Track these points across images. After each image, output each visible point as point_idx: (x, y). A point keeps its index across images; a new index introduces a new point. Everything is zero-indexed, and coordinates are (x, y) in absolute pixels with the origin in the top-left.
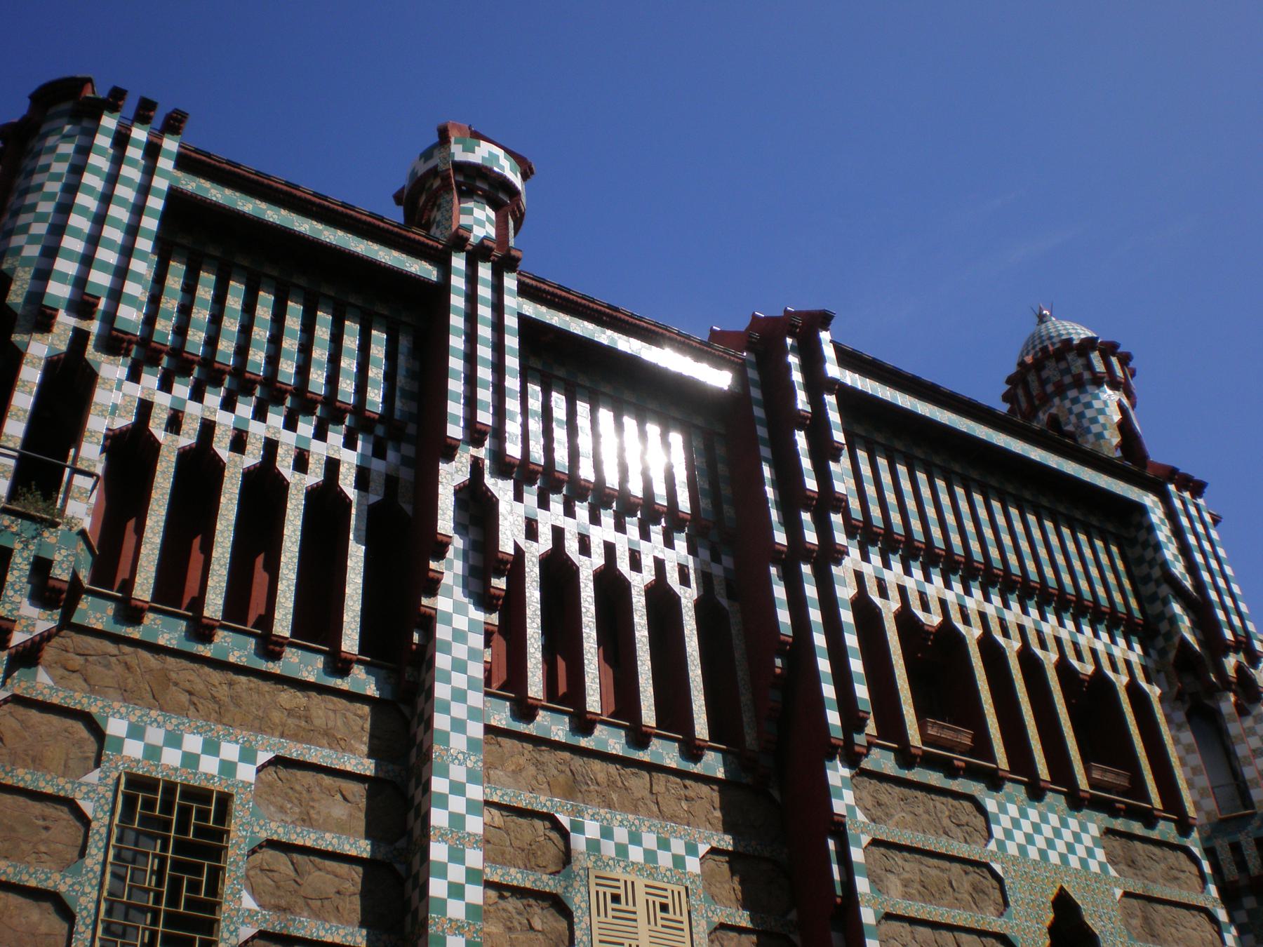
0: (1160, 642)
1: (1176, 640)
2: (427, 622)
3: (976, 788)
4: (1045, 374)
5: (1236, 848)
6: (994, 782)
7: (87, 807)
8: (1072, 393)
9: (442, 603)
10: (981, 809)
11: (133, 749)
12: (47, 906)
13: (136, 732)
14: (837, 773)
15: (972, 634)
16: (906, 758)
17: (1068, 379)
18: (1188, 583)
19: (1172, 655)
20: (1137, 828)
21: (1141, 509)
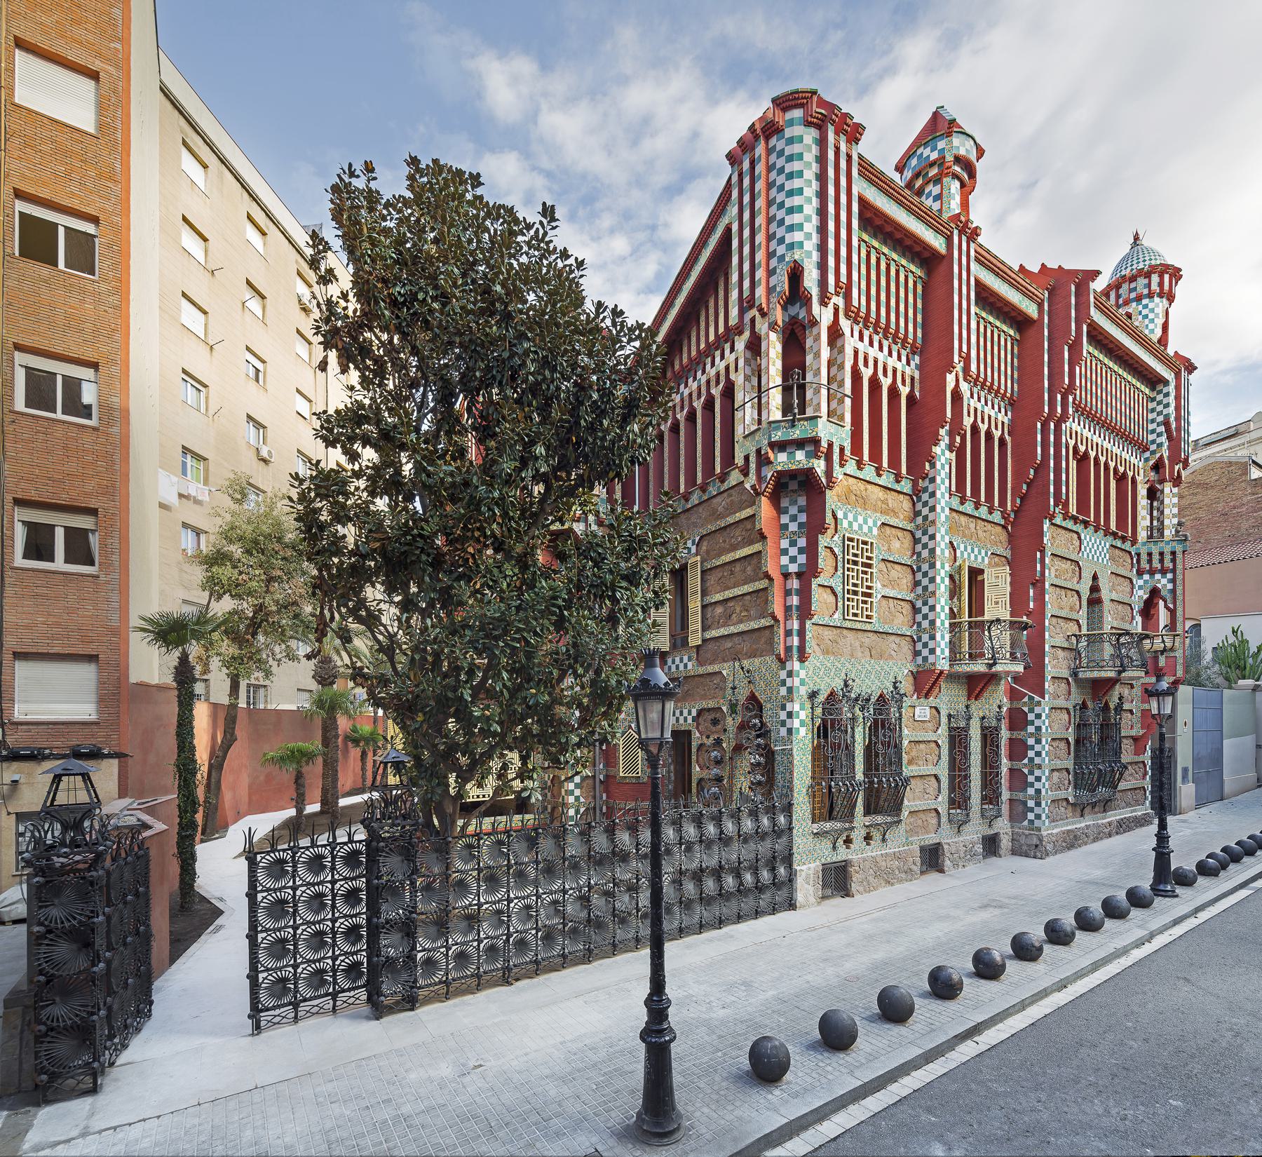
0: (1147, 454)
1: (1158, 455)
2: (932, 461)
3: (1079, 528)
4: (1133, 285)
5: (1150, 554)
6: (1086, 524)
7: (836, 550)
8: (1145, 301)
9: (937, 450)
10: (1079, 538)
11: (845, 524)
12: (829, 591)
13: (846, 516)
14: (1046, 526)
15: (1092, 454)
16: (1066, 516)
17: (1146, 291)
18: (1174, 426)
19: (1151, 463)
20: (1119, 543)
21: (1166, 383)
